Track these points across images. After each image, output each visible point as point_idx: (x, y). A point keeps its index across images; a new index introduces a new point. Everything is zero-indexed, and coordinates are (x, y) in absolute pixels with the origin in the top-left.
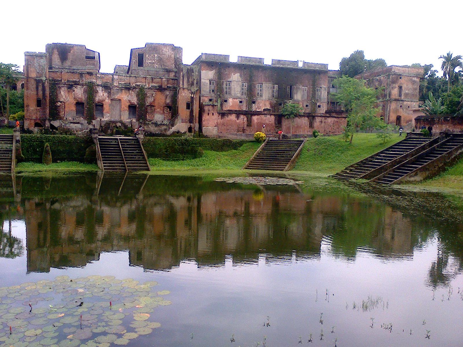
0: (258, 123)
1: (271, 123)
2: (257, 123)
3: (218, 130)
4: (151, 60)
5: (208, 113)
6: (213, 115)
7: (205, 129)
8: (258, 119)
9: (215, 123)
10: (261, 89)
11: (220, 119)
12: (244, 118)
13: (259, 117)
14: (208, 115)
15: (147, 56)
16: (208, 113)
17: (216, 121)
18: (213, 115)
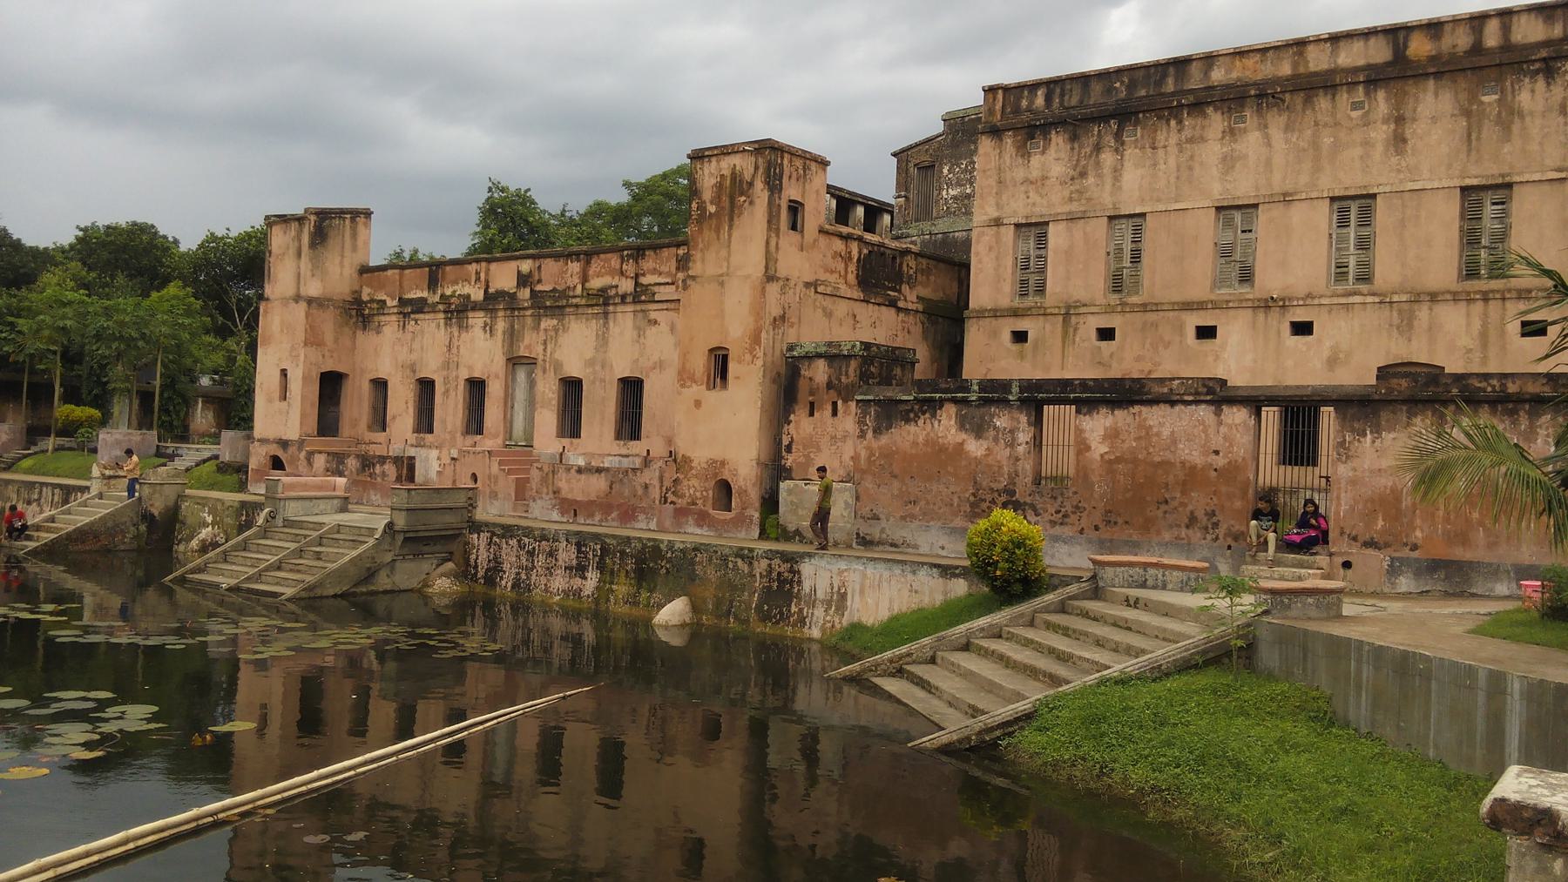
0: (1118, 460)
1: (1220, 461)
2: (1109, 464)
3: (857, 498)
4: (959, 184)
5: (812, 404)
6: (835, 413)
7: (790, 492)
8: (1112, 435)
9: (847, 457)
10: (1365, 232)
11: (870, 434)
12: (1012, 432)
13: (1121, 417)
14: (812, 414)
15: (945, 171)
16: (812, 404)
17: (848, 450)
18: (835, 413)
